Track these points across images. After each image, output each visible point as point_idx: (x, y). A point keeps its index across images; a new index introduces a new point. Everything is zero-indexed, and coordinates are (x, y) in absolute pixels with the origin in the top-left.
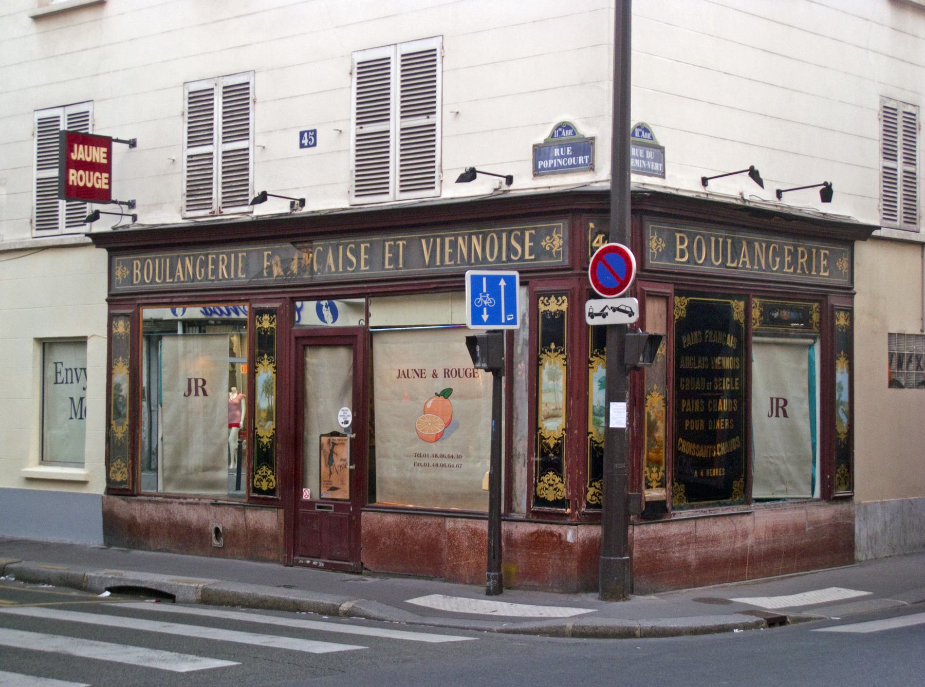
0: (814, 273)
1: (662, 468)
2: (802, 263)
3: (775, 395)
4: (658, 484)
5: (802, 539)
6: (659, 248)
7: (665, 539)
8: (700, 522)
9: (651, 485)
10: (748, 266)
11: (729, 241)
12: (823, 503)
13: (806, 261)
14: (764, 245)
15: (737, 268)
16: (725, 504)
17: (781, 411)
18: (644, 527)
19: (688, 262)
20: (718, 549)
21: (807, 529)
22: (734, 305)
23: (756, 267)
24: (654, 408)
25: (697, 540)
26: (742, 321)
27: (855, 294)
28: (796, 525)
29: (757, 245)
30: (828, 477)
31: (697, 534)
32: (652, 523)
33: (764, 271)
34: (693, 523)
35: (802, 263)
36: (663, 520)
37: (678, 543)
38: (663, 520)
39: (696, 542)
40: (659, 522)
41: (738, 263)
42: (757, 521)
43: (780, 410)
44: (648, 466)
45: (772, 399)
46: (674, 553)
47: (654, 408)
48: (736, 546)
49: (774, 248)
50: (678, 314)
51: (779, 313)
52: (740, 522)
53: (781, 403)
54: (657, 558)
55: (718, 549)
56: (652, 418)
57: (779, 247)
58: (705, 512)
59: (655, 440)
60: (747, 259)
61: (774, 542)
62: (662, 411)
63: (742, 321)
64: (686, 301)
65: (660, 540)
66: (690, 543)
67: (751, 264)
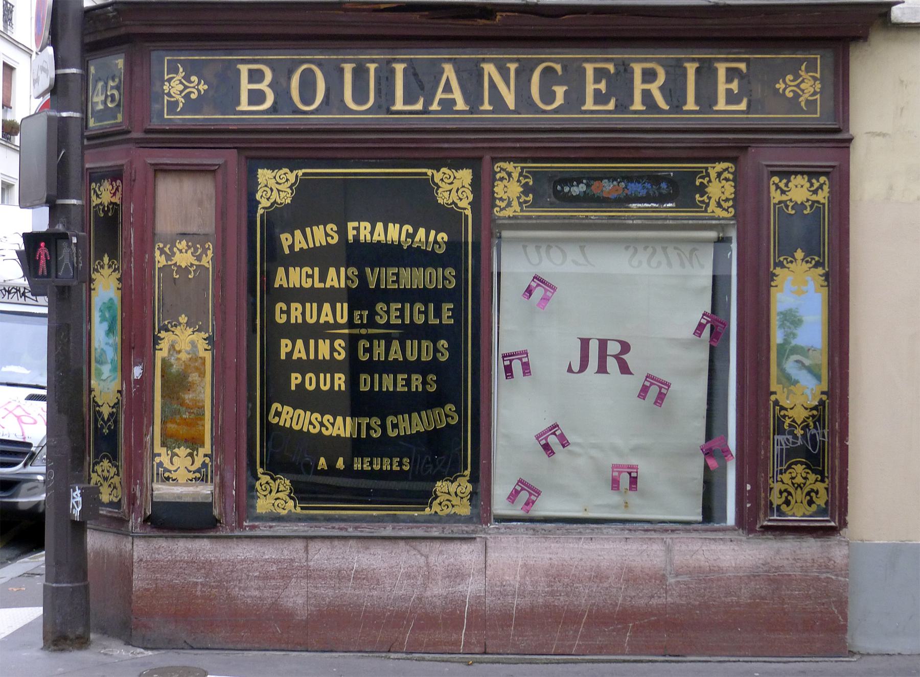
0: (691, 105)
1: (207, 448)
2: (647, 95)
3: (595, 333)
4: (191, 476)
5: (652, 597)
6: (190, 92)
7: (221, 565)
8: (314, 546)
9: (174, 476)
10: (461, 105)
11: (399, 68)
12: (741, 535)
13: (661, 89)
14: (513, 67)
15: (425, 111)
16: (413, 520)
17: (612, 364)
18: (163, 543)
19: (274, 109)
20: (375, 593)
21: (672, 580)
22: (438, 176)
23: (487, 106)
24: (179, 352)
25: (309, 575)
26: (464, 204)
27: (850, 140)
28: (630, 570)
29: (490, 69)
30: (749, 487)
31: (311, 564)
32: (161, 537)
33: (514, 112)
34: (299, 545)
35: (647, 95)
36: (212, 534)
37: (257, 574)
38: (212, 534)
39: (308, 577)
40: (203, 537)
41: (429, 102)
42: (493, 556)
43: (612, 364)
44: (163, 444)
45: (585, 343)
46: (245, 589)
47: (179, 352)
48: (428, 593)
49: (548, 71)
50: (268, 199)
51: (588, 185)
52: (441, 552)
53: (613, 348)
54: (199, 593)
55: (375, 593)
56: (174, 369)
57: (564, 68)
58: (341, 529)
59: (182, 404)
60: (457, 94)
61: (552, 594)
62: (204, 359)
63: (464, 204)
64: (292, 177)
65: (207, 566)
66: (290, 578)
67: (467, 101)
